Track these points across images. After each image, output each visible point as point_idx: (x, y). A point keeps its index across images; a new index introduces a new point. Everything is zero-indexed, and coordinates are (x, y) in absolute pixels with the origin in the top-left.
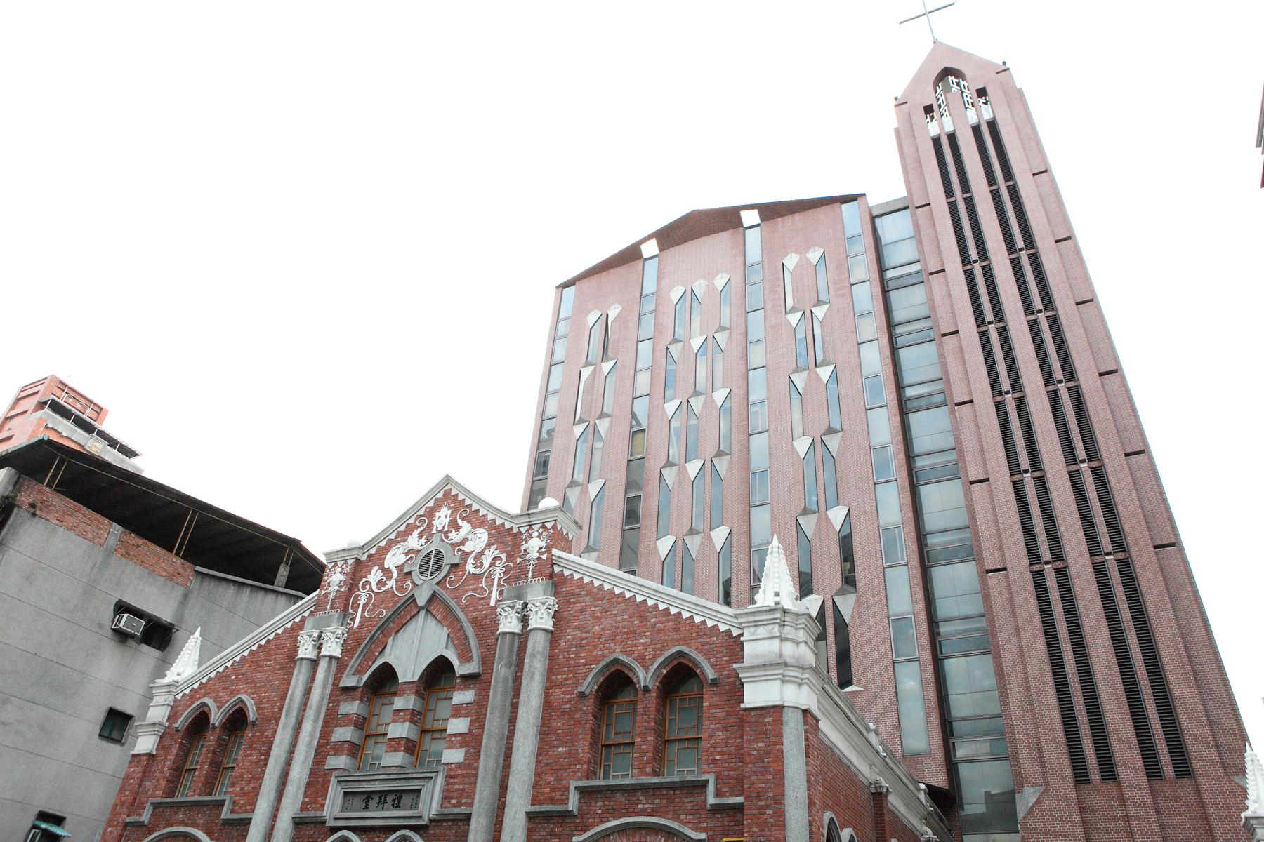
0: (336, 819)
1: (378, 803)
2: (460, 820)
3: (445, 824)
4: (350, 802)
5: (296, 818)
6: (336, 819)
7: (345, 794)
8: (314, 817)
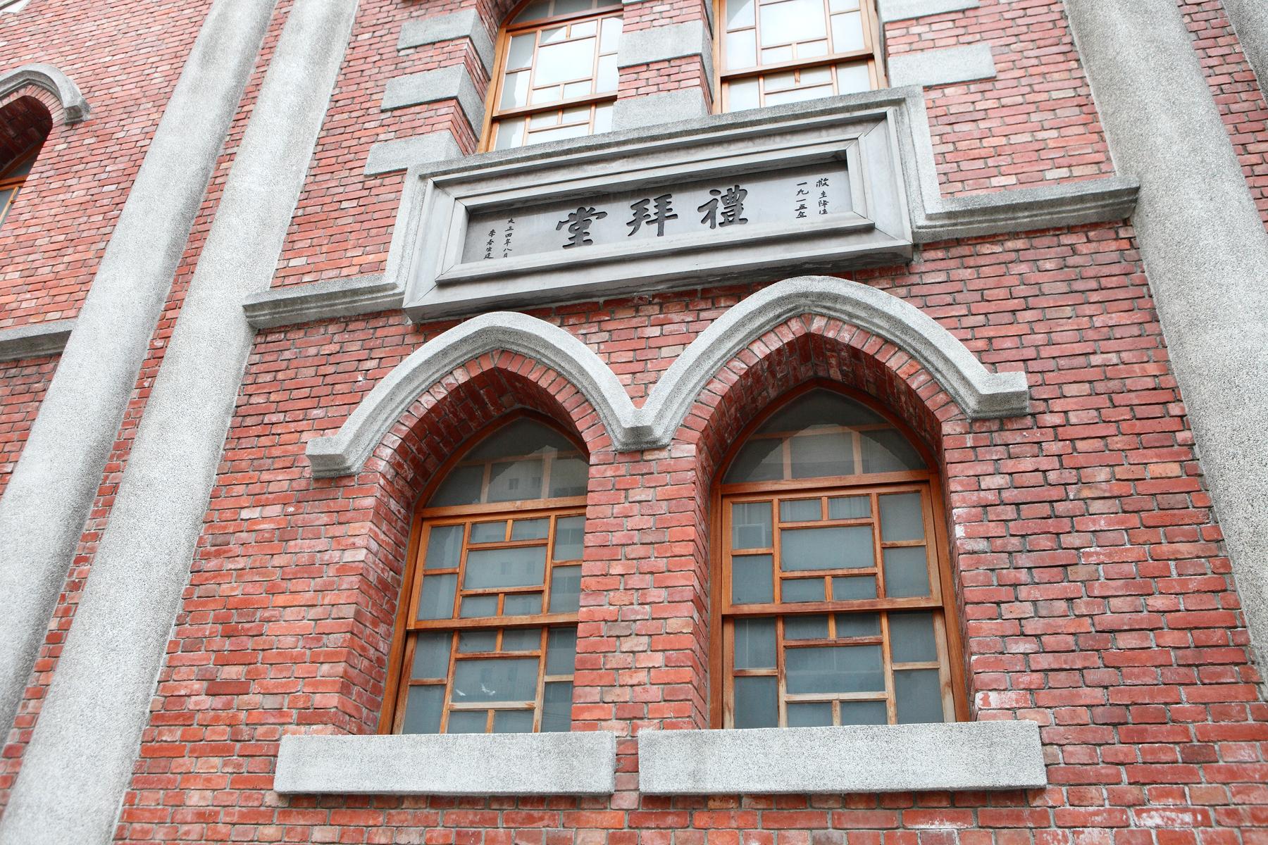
0: (443, 285)
1: (634, 224)
2: (1071, 229)
3: (986, 248)
4: (500, 238)
5: (261, 306)
6: (443, 285)
7: (475, 215)
8: (344, 294)
